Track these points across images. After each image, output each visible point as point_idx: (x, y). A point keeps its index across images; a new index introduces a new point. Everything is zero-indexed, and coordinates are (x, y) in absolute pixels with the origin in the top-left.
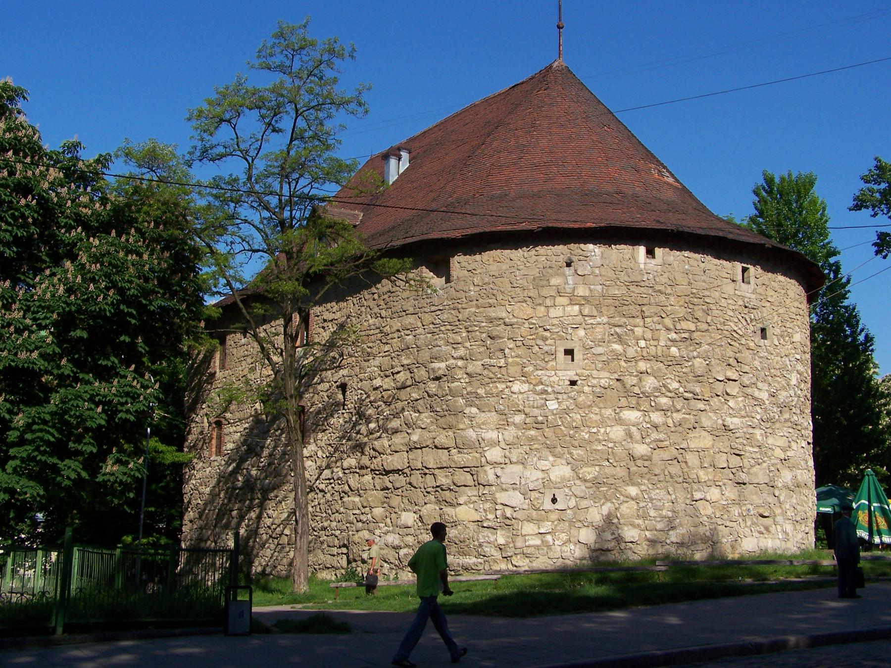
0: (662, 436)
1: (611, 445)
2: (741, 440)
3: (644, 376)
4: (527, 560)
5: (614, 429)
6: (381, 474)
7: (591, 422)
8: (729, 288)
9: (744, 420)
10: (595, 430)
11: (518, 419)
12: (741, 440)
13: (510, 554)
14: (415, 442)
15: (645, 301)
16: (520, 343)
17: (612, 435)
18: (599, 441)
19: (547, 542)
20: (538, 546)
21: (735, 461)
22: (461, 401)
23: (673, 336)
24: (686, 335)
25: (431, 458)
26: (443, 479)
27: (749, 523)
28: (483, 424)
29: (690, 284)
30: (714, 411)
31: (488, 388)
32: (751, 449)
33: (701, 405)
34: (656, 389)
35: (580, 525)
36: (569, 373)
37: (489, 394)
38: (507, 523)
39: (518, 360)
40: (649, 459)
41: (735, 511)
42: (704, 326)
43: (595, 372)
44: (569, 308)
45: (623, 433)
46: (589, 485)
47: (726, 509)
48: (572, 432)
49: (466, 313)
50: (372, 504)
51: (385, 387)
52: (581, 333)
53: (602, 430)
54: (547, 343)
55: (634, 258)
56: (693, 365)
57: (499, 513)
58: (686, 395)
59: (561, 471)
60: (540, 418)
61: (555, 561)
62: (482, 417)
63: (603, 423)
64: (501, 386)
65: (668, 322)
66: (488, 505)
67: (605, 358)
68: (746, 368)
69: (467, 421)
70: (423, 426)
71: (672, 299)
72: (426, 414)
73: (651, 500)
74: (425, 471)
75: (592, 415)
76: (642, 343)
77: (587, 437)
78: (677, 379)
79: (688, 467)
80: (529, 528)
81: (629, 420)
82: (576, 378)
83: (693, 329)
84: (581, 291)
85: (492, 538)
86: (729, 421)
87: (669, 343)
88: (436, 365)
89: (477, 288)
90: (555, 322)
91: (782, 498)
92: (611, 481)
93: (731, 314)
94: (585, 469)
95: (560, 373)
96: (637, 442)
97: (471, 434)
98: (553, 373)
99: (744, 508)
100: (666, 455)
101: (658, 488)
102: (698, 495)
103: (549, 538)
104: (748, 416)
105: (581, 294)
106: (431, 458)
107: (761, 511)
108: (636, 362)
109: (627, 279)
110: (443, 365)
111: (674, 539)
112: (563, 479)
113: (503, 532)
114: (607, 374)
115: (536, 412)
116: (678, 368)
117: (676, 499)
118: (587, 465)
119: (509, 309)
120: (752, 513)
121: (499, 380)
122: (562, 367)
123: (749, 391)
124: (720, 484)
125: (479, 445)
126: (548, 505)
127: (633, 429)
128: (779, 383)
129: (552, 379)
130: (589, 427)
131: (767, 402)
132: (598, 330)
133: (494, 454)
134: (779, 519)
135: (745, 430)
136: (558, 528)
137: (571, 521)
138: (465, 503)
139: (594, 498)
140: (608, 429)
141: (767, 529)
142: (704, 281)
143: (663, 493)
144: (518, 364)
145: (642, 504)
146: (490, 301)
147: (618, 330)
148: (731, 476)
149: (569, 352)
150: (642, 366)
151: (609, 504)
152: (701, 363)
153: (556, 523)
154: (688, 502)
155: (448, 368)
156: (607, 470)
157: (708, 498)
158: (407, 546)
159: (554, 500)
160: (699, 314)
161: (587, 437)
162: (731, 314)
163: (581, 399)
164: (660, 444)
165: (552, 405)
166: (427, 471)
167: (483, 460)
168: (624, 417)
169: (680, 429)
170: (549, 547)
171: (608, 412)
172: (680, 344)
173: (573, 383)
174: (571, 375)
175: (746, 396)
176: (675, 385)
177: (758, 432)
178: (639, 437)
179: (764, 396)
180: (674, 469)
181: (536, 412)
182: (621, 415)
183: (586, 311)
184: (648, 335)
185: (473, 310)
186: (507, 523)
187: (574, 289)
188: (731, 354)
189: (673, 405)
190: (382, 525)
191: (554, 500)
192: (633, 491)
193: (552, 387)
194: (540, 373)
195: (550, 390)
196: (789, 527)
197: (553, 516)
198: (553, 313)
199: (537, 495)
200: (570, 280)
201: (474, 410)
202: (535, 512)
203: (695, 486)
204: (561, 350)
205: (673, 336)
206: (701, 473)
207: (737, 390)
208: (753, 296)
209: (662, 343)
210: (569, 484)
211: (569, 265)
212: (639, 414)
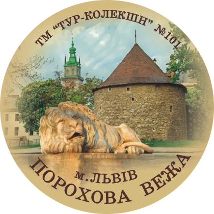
86: (124, 117)
150: (109, 109)
177: (131, 118)
179: (133, 111)
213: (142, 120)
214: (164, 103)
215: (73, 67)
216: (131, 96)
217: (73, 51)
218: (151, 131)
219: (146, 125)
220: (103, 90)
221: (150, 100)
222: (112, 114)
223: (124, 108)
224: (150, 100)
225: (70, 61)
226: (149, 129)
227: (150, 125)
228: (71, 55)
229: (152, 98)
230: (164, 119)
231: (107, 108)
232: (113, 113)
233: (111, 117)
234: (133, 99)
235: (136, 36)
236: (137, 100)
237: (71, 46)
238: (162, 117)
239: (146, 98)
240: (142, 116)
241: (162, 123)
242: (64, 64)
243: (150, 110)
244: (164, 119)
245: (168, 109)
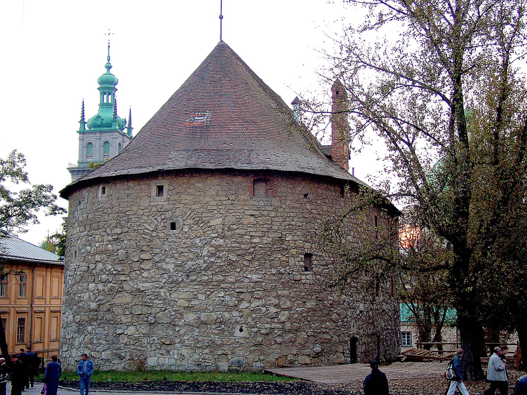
9: (154, 284)
21: (145, 310)
23: (110, 238)
24: (115, 237)
27: (154, 348)
32: (158, 302)
33: (123, 278)
34: (102, 270)
41: (145, 340)
46: (77, 325)
52: (79, 242)
58: (114, 272)
68: (157, 251)
84: (81, 219)
86: (141, 286)
87: (108, 243)
93: (146, 218)
99: (151, 339)
102: (119, 331)
117: (108, 333)
120: (156, 342)
123: (159, 265)
131: (172, 271)
132: (84, 239)
135: (153, 290)
139: (78, 332)
141: (168, 352)
147: (90, 238)
148: (145, 319)
149: (76, 252)
150: (98, 257)
160: (123, 222)
162: (146, 218)
164: (102, 302)
169: (111, 292)
171: (85, 284)
172: (113, 242)
176: (110, 267)
177: (162, 291)
179: (171, 267)
180: (108, 317)
192: (90, 328)
206: (123, 318)
212: (94, 285)
213: (202, 297)
214: (281, 240)
215: (106, 137)
216: (168, 215)
217: (108, 86)
218: (232, 334)
219: (214, 316)
220: (85, 192)
221: (229, 229)
222: (104, 276)
223: (143, 256)
224: (229, 229)
225: (98, 117)
226: (223, 330)
227: (227, 315)
228: (102, 99)
229: (239, 222)
230: (278, 297)
233: (100, 287)
234: (173, 226)
235: (221, 17)
236: (186, 229)
237: (105, 71)
238: (275, 288)
239: (217, 222)
240: (200, 283)
241: (273, 310)
242: (78, 127)
243: (231, 263)
244: (278, 297)
245: (298, 262)
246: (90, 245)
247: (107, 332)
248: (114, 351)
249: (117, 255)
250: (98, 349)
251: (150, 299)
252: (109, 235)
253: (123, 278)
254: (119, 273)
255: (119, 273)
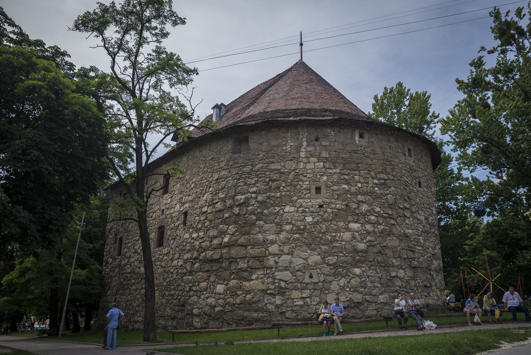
0: (372, 239)
1: (344, 243)
2: (413, 243)
3: (361, 204)
4: (295, 315)
5: (346, 234)
6: (206, 262)
7: (332, 230)
8: (402, 158)
10: (334, 234)
11: (288, 227)
12: (413, 243)
13: (284, 310)
14: (225, 243)
15: (360, 161)
16: (289, 184)
17: (344, 238)
18: (337, 241)
19: (307, 302)
20: (301, 305)
21: (410, 254)
22: (254, 217)
23: (376, 181)
25: (234, 252)
26: (242, 265)
27: (420, 290)
28: (267, 230)
29: (383, 153)
30: (399, 225)
31: (270, 210)
33: (392, 222)
34: (368, 211)
35: (327, 292)
36: (318, 200)
37: (271, 213)
38: (281, 292)
39: (288, 193)
40: (366, 252)
41: (413, 283)
42: (392, 177)
43: (333, 200)
44: (317, 164)
45: (351, 236)
47: (407, 282)
48: (321, 235)
49: (257, 167)
50: (200, 280)
51: (209, 211)
52: (325, 178)
53: (339, 234)
54: (305, 183)
55: (353, 138)
56: (387, 198)
57: (277, 284)
59: (315, 258)
60: (302, 227)
61: (312, 315)
62: (267, 226)
63: (338, 230)
64: (277, 209)
65: (372, 173)
66: (270, 280)
67: (339, 193)
68: (413, 203)
69: (257, 229)
70: (231, 233)
71: (374, 161)
72: (233, 226)
73: (368, 276)
74: (232, 260)
75: (332, 226)
76: (359, 185)
77: (330, 238)
78: (379, 206)
79: (388, 257)
80: (295, 294)
81: (354, 229)
82: (322, 203)
83: (386, 178)
84: (324, 154)
85: (273, 300)
88: (239, 197)
89: (264, 153)
90: (309, 171)
91: (434, 276)
92: (345, 265)
93: (404, 172)
94: (329, 258)
95: (313, 201)
96: (358, 242)
97: (260, 236)
98: (309, 200)
100: (375, 250)
101: (371, 270)
102: (394, 274)
103: (308, 300)
104: (415, 229)
105: (324, 156)
106: (234, 252)
107: (425, 283)
108: (357, 195)
109: (349, 149)
110: (243, 197)
111: (382, 301)
112: (316, 264)
113: (280, 297)
114: (340, 202)
115: (299, 223)
116: (379, 200)
118: (329, 256)
119: (282, 164)
121: (277, 205)
122: (314, 197)
124: (404, 267)
125: (265, 243)
126: (307, 280)
127: (356, 234)
128: (428, 212)
129: (308, 204)
130: (331, 232)
133: (274, 248)
134: (434, 288)
136: (314, 294)
137: (321, 289)
138: (256, 279)
139: (335, 275)
140: (342, 234)
141: (429, 294)
142: (390, 153)
143: (374, 272)
144: (288, 195)
145: (363, 279)
146: (272, 160)
147: (346, 177)
148: (409, 263)
150: (360, 198)
151: (344, 279)
152: (391, 197)
153: (312, 291)
154: (388, 278)
155: (247, 199)
156: (342, 258)
157: (399, 276)
158: (220, 305)
159: (311, 277)
160: (389, 170)
161: (330, 238)
162: (404, 172)
163: (325, 216)
165: (309, 219)
166: (232, 260)
167: (267, 252)
168: (350, 227)
169: (382, 235)
170: (308, 306)
171: (341, 224)
173: (321, 206)
174: (319, 201)
175: (414, 218)
176: (378, 209)
177: (421, 238)
178: (359, 239)
180: (380, 258)
181: (299, 223)
182: (349, 225)
183: (327, 166)
184: (362, 180)
185: (261, 165)
186: (281, 292)
187: (320, 153)
188: (405, 194)
189: (378, 221)
190: (204, 293)
191: (311, 277)
192: (357, 271)
193: (308, 208)
194: (301, 200)
195: (307, 210)
196: (439, 293)
197: (310, 287)
198: (309, 166)
199: (301, 274)
200: (318, 148)
201: (262, 223)
202: (299, 285)
203: (391, 269)
204: (314, 187)
205: (376, 181)
206: (394, 261)
207: (409, 214)
208: (414, 164)
209: (370, 185)
210: (319, 267)
211: (316, 140)
212: (359, 225)
222: (373, 218)
231: (355, 194)
232: (379, 215)
233: (369, 227)
235: (301, 45)
246: (348, 183)
247: (380, 274)
248: (392, 294)
249: (386, 199)
250: (374, 292)
251: (414, 245)
252: (373, 178)
253: (392, 222)
254: (390, 217)
255: (390, 217)
